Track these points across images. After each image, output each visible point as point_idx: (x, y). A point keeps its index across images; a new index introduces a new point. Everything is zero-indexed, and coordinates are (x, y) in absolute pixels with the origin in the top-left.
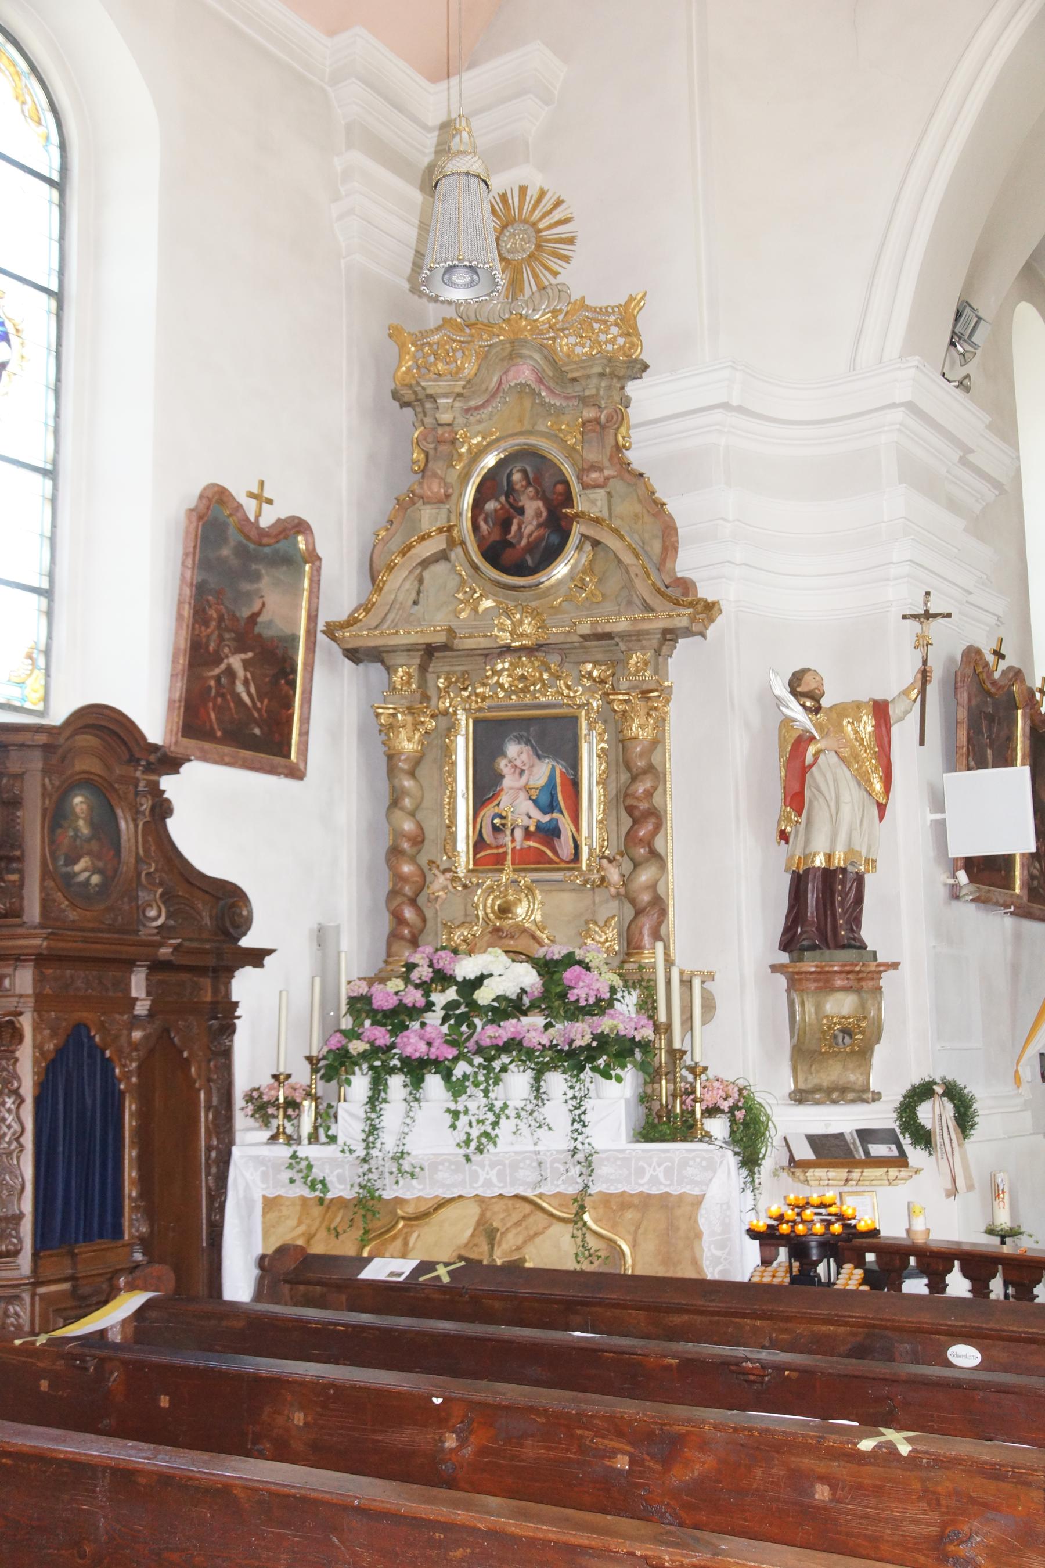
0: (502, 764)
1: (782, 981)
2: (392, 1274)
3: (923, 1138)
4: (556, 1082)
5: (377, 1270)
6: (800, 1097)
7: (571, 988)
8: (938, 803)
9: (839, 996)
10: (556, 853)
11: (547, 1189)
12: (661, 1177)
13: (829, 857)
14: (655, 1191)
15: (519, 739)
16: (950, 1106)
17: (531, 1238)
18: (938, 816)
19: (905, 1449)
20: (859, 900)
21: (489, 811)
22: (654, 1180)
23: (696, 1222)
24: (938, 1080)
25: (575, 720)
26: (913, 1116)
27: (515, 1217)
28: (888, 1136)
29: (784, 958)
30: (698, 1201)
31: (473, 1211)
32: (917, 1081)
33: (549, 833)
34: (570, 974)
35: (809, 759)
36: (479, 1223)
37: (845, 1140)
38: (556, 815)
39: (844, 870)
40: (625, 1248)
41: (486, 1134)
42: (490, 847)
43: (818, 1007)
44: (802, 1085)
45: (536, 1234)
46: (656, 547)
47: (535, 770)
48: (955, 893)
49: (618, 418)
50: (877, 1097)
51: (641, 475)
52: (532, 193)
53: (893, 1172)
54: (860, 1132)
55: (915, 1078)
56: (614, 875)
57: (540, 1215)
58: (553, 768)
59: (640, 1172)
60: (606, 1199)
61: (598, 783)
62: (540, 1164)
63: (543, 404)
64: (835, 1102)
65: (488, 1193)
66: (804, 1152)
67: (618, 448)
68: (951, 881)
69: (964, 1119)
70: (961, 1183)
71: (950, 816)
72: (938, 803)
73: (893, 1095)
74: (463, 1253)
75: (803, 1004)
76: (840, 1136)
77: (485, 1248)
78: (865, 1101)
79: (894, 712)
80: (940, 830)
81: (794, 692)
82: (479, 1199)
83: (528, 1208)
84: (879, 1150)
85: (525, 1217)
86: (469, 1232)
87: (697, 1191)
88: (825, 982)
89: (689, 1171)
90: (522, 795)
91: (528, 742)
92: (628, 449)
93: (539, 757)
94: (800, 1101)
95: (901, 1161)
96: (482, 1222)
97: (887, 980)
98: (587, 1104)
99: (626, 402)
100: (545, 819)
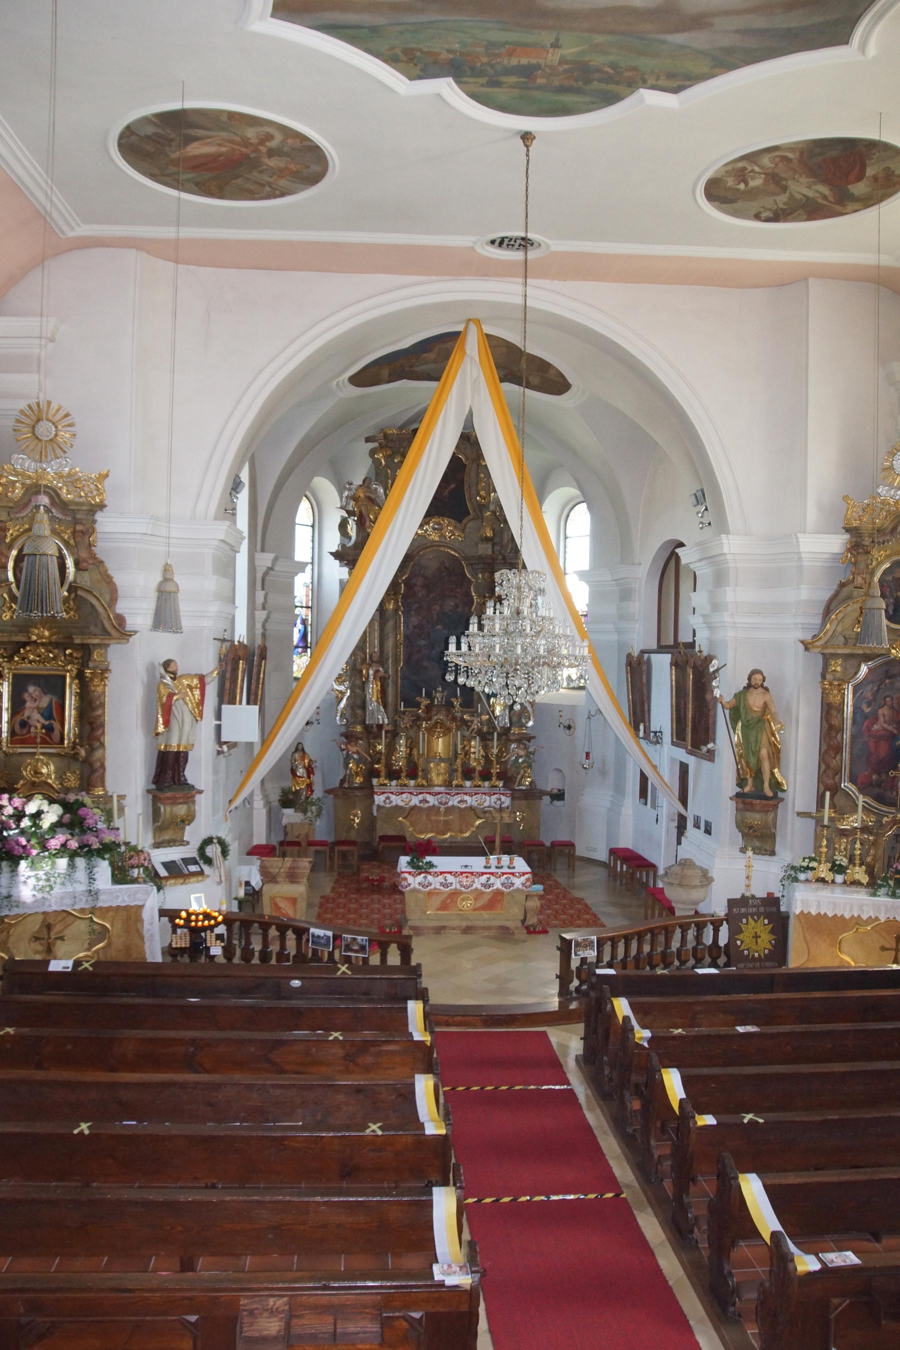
0: (26, 696)
1: (151, 797)
2: (64, 968)
3: (209, 861)
4: (80, 862)
5: (55, 966)
6: (157, 845)
7: (85, 819)
8: (219, 716)
9: (181, 806)
10: (51, 739)
11: (77, 907)
12: (126, 899)
13: (179, 746)
14: (123, 905)
15: (35, 684)
16: (218, 846)
17: (67, 927)
18: (218, 722)
19: (341, 1038)
20: (186, 762)
21: (18, 718)
22: (124, 901)
23: (140, 915)
24: (214, 836)
25: (64, 677)
26: (204, 852)
27: (59, 918)
28: (193, 861)
29: (154, 787)
30: (142, 906)
31: (40, 918)
32: (206, 837)
33: (49, 729)
34: (82, 812)
35: (173, 702)
36: (43, 922)
37: (176, 864)
38: (52, 721)
39: (183, 752)
40: (108, 926)
41: (50, 886)
42: (17, 735)
43: (172, 810)
44: (158, 841)
45: (69, 925)
46: (108, 597)
47: (42, 699)
48: (219, 753)
49: (90, 531)
50: (188, 843)
51: (102, 562)
52: (55, 406)
53: (200, 878)
54: (183, 860)
55: (204, 835)
56: (83, 753)
57: (71, 917)
58: (51, 699)
59: (118, 897)
60: (101, 908)
61: (74, 709)
62: (75, 897)
63: (53, 517)
64: (171, 846)
65: (50, 910)
66: (163, 872)
67: (90, 545)
68: (220, 749)
69: (225, 853)
70: (223, 878)
71: (224, 722)
72: (219, 716)
73: (196, 843)
74: (36, 935)
75: (165, 810)
76: (174, 862)
77: (45, 931)
78: (184, 845)
79: (207, 680)
80: (218, 728)
81: (166, 671)
82: (44, 913)
83: (65, 915)
84: (193, 868)
85: (64, 918)
86: (38, 926)
87: (140, 903)
88: (174, 802)
89: (138, 896)
90: (36, 711)
91: (39, 686)
92: (95, 546)
93: (45, 694)
94: (158, 848)
95: (201, 873)
96: (44, 920)
97: (198, 797)
98: (95, 870)
99: (94, 522)
100: (47, 723)
